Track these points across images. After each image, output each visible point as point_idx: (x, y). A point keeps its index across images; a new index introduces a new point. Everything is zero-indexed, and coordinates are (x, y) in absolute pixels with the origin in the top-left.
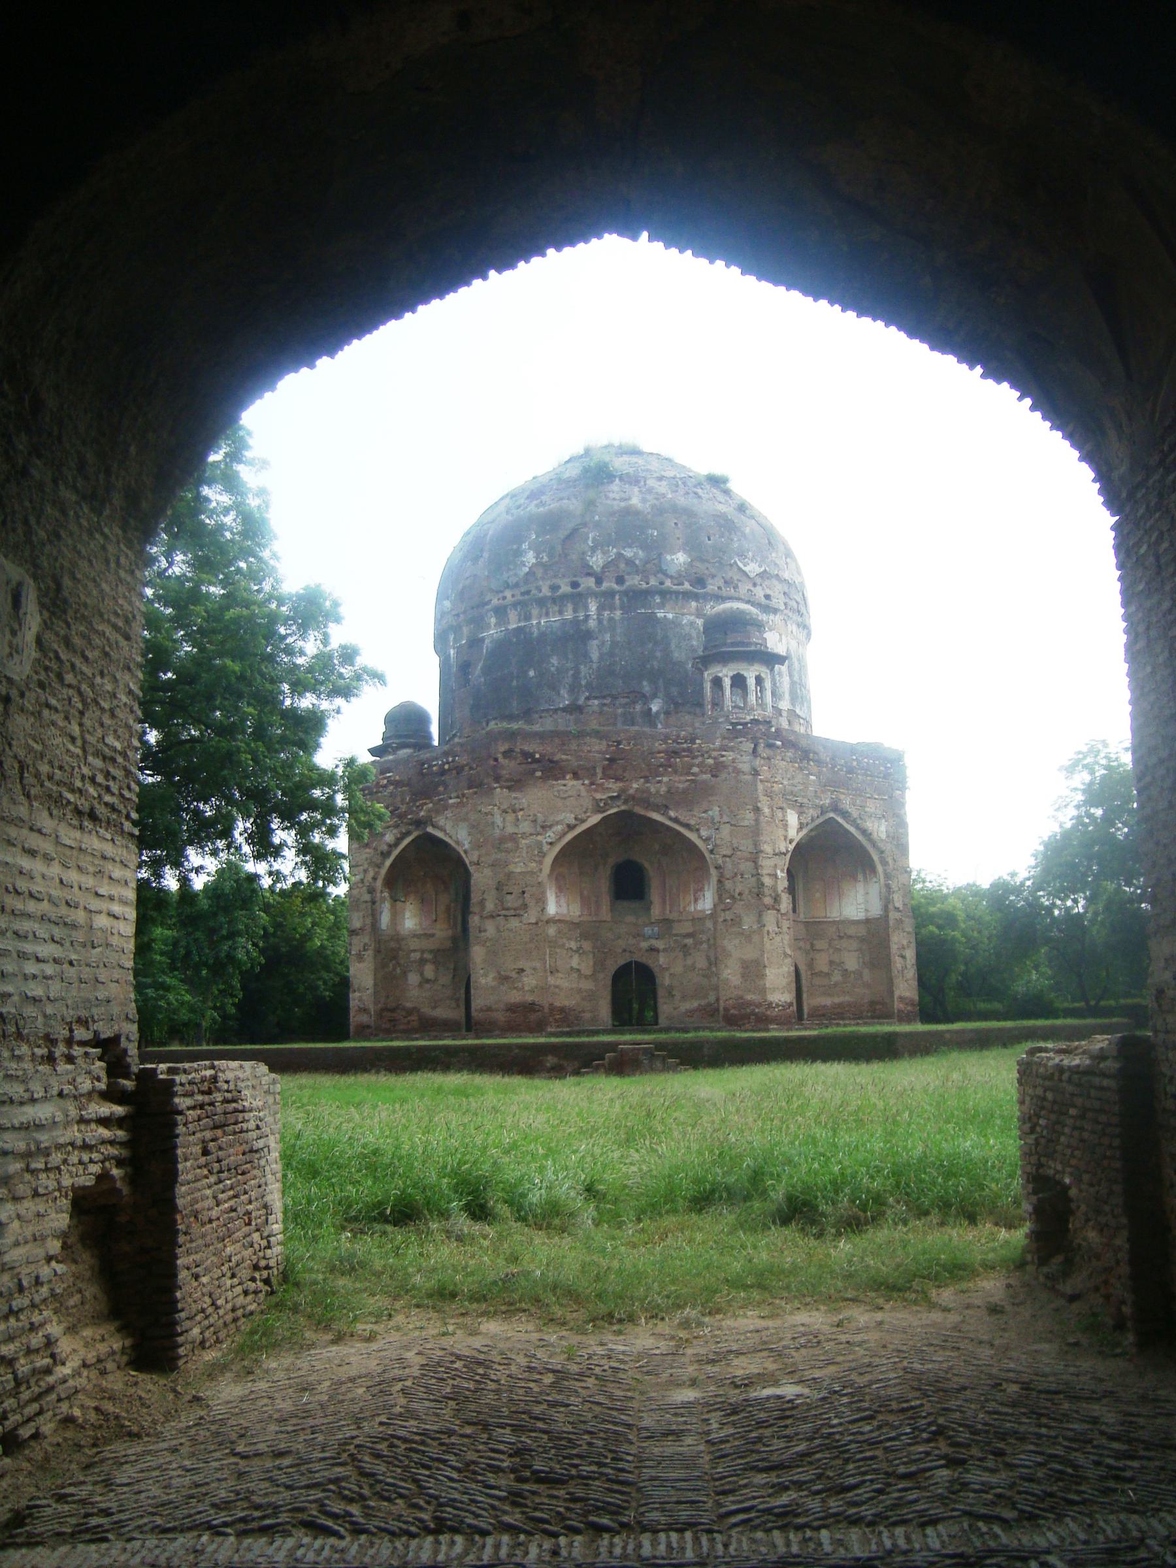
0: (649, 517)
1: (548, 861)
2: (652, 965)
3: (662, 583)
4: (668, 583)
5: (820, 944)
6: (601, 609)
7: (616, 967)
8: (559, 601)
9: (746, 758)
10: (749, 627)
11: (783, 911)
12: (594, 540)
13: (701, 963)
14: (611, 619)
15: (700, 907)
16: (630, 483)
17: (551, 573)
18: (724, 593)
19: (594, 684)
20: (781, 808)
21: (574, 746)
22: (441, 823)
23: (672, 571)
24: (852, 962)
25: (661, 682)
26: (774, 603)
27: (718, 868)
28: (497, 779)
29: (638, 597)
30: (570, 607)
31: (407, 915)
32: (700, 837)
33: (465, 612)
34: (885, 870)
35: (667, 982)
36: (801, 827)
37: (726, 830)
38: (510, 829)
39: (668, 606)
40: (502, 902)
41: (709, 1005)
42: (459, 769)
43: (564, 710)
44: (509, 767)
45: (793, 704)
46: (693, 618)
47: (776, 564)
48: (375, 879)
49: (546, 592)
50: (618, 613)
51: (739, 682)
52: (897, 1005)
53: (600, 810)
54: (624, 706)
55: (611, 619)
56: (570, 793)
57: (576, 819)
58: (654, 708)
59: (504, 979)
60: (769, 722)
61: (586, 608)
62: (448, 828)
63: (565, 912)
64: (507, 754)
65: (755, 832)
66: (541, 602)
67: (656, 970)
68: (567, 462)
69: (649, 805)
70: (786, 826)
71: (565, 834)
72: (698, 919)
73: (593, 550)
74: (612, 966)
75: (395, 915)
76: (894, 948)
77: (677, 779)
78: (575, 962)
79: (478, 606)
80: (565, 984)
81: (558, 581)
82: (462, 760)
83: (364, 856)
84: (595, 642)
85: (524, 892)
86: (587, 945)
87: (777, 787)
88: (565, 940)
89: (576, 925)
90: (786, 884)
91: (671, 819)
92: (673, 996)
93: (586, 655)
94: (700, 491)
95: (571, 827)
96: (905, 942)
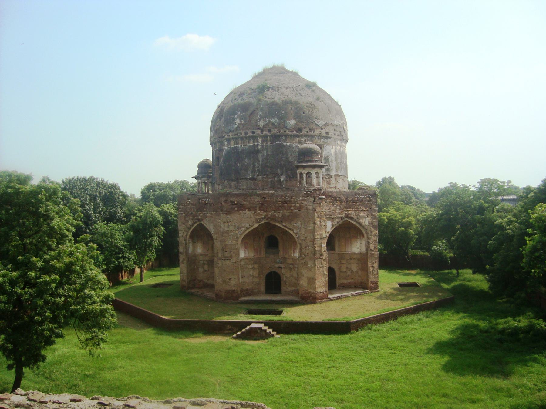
1: (240, 240)
2: (279, 273)
3: (285, 132)
5: (343, 261)
6: (263, 142)
7: (267, 273)
9: (311, 204)
10: (313, 154)
11: (324, 258)
12: (260, 115)
13: (295, 275)
14: (266, 146)
15: (295, 255)
16: (275, 91)
17: (245, 128)
18: (310, 133)
19: (260, 170)
20: (325, 221)
21: (249, 199)
22: (205, 222)
23: (289, 127)
24: (355, 268)
26: (330, 135)
27: (300, 244)
28: (222, 211)
29: (276, 137)
30: (252, 141)
31: (198, 248)
32: (294, 233)
33: (217, 138)
34: (367, 236)
35: (284, 279)
36: (333, 226)
37: (303, 231)
38: (226, 229)
39: (288, 140)
40: (223, 254)
41: (297, 290)
42: (210, 204)
43: (250, 179)
44: (226, 206)
45: (337, 172)
46: (297, 144)
47: (331, 119)
48: (186, 236)
49: (243, 135)
50: (269, 143)
52: (370, 285)
53: (258, 222)
54: (271, 178)
55: (266, 146)
56: (247, 216)
57: (249, 225)
58: (282, 179)
59: (224, 281)
60: (321, 189)
61: (258, 142)
62: (207, 224)
63: (248, 255)
64: (225, 201)
65: (314, 231)
66: (242, 138)
67: (281, 275)
69: (276, 221)
70: (326, 227)
71: (246, 230)
72: (294, 259)
73: (260, 119)
74: (266, 272)
75: (194, 248)
76: (369, 264)
77: (285, 211)
78: (251, 273)
79: (221, 137)
80: (247, 281)
81: (247, 131)
82: (211, 201)
83: (183, 227)
84: (261, 154)
85: (231, 251)
86: (256, 266)
87: (322, 214)
88: (247, 266)
89: (251, 260)
90: (326, 248)
91: (283, 226)
92: (287, 284)
93: (258, 159)
94: (302, 92)
95: (248, 228)
96: (374, 262)
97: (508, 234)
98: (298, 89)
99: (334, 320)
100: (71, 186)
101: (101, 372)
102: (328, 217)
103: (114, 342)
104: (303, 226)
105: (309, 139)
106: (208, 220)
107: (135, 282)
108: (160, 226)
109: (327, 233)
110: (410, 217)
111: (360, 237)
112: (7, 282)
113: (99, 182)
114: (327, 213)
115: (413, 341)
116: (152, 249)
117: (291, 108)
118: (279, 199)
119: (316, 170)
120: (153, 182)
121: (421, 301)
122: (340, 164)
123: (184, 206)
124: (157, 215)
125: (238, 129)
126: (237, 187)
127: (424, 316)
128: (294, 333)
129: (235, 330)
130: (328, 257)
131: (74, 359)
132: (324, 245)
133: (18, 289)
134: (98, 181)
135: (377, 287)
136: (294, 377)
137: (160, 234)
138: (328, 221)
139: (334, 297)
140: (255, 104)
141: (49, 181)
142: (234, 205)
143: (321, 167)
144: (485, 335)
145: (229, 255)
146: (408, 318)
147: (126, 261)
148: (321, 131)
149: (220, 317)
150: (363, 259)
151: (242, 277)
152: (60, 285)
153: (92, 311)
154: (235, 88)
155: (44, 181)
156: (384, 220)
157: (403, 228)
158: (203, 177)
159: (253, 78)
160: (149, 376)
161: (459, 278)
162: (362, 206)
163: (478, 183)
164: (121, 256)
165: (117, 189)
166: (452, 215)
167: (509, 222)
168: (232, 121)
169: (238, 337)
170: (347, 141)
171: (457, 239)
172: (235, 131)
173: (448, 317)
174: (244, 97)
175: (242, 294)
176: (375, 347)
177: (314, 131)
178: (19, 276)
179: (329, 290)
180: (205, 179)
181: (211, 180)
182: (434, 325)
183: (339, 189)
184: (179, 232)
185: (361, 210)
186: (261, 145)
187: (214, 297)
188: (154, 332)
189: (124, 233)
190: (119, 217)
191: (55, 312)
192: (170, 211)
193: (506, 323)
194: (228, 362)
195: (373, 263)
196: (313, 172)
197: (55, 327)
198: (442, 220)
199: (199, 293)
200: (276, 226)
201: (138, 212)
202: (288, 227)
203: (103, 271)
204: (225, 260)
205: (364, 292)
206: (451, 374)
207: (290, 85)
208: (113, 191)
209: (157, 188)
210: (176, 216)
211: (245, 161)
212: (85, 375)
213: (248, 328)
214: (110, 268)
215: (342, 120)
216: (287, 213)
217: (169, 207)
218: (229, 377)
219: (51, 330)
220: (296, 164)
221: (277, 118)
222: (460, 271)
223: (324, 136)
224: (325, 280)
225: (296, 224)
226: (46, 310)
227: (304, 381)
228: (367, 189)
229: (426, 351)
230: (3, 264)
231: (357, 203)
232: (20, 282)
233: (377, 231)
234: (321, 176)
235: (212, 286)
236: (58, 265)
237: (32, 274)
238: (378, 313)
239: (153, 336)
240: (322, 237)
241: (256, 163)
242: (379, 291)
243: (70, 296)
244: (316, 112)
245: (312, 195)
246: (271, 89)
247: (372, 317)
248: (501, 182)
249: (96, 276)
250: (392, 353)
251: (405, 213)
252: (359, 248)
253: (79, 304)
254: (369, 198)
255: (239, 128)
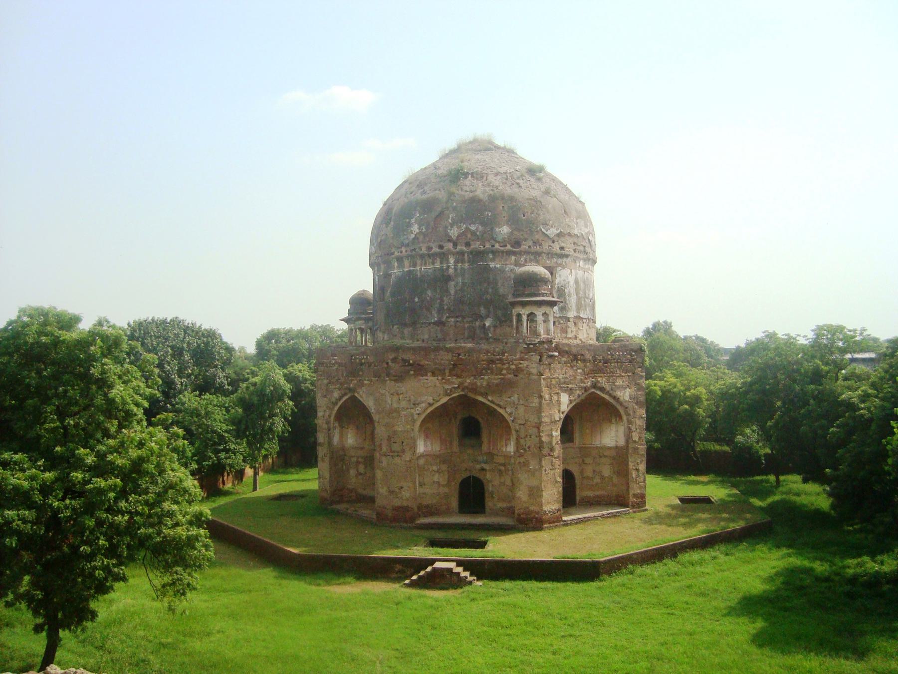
0: (487, 203)
1: (418, 423)
2: (482, 479)
3: (493, 246)
4: (497, 246)
5: (588, 460)
6: (456, 262)
7: (462, 479)
8: (432, 256)
9: (535, 365)
10: (539, 283)
11: (556, 455)
13: (508, 482)
14: (462, 268)
15: (508, 450)
16: (477, 179)
18: (533, 249)
20: (558, 393)
21: (432, 356)
22: (361, 393)
23: (500, 238)
24: (607, 471)
25: (491, 309)
26: (566, 252)
27: (517, 431)
28: (388, 375)
29: (478, 255)
30: (438, 260)
31: (349, 436)
34: (628, 419)
35: (490, 489)
36: (571, 401)
37: (521, 410)
38: (395, 405)
39: (497, 260)
40: (390, 447)
41: (512, 507)
43: (435, 323)
44: (395, 367)
45: (578, 310)
46: (512, 266)
48: (330, 416)
49: (424, 250)
50: (467, 265)
51: (531, 317)
52: (632, 499)
53: (447, 395)
54: (469, 322)
55: (462, 268)
57: (433, 400)
58: (487, 324)
59: (391, 492)
60: (551, 341)
61: (448, 262)
62: (364, 396)
63: (429, 448)
64: (394, 360)
65: (539, 410)
66: (422, 256)
68: (446, 156)
70: (560, 404)
71: (427, 409)
72: (507, 457)
73: (452, 227)
74: (459, 479)
76: (631, 465)
78: (436, 478)
81: (431, 245)
82: (371, 359)
84: (453, 283)
85: (403, 442)
86: (444, 467)
89: (437, 456)
90: (559, 438)
91: (489, 401)
93: (447, 291)
94: (521, 182)
95: (430, 405)
97: (862, 416)
98: (515, 177)
99: (573, 557)
100: (142, 332)
101: (188, 639)
102: (564, 388)
103: (209, 590)
104: (521, 402)
105: (532, 257)
106: (364, 390)
107: (245, 491)
108: (286, 400)
109: (561, 413)
110: (699, 388)
111: (616, 420)
112: (37, 488)
113: (188, 327)
114: (562, 381)
115: (703, 594)
116: (273, 438)
117: (503, 207)
118: (483, 357)
119: (544, 309)
120: (276, 327)
121: (717, 528)
122: (583, 299)
123: (327, 367)
124: (282, 381)
125: (416, 241)
126: (412, 338)
127: (722, 553)
128: (505, 579)
129: (409, 573)
130: (564, 453)
131: (142, 616)
132: (557, 434)
133: (55, 500)
134: (187, 324)
135: (645, 502)
136: (505, 652)
137: (287, 412)
138: (562, 394)
139: (573, 520)
140: (445, 199)
141: (108, 325)
142: (408, 365)
143: (552, 304)
144: (824, 585)
145: (399, 449)
146: (695, 556)
147: (229, 457)
148: (552, 244)
149: (384, 550)
150: (620, 456)
151: (421, 485)
152: (123, 494)
153: (174, 539)
154: (411, 174)
155: (100, 324)
156: (655, 392)
157: (686, 407)
158: (359, 319)
159: (440, 158)
160: (266, 648)
161: (781, 489)
162: (619, 369)
163: (812, 331)
164: (221, 447)
165: (217, 339)
166: (769, 384)
167: (864, 396)
168: (405, 228)
169: (413, 585)
170: (594, 262)
171: (777, 423)
172: (410, 244)
173: (761, 555)
174: (426, 188)
175: (420, 513)
176: (640, 603)
177: (541, 245)
178: (57, 480)
179: (563, 507)
180: (360, 324)
181: (370, 324)
182: (738, 568)
183: (580, 340)
184: (318, 411)
185: (617, 375)
186: (453, 267)
187: (374, 516)
188: (274, 574)
189: (228, 411)
190: (219, 384)
191: (114, 539)
192: (303, 375)
193: (859, 565)
194: (396, 626)
195: (638, 464)
196: (539, 312)
197: (113, 564)
198: (751, 394)
199: (349, 511)
200: (476, 401)
201: (250, 376)
202: (498, 403)
203: (193, 473)
204: (392, 456)
205: (621, 511)
206: (767, 651)
207: (502, 170)
208: (210, 342)
209: (283, 338)
210: (312, 384)
211: (426, 294)
212: (160, 643)
213: (429, 569)
214: (204, 468)
215: (586, 227)
216: (494, 379)
217: (303, 369)
218: (397, 650)
219: (107, 569)
220: (511, 299)
221: (482, 224)
222: (782, 478)
223: (556, 254)
224: (558, 493)
225: (509, 398)
226: (99, 535)
227: (523, 658)
228: (628, 341)
229: (725, 612)
230: (30, 459)
231: (611, 363)
232: (57, 489)
233: (644, 411)
234: (551, 319)
235: (372, 500)
236: (120, 462)
237: (77, 476)
238: (644, 548)
239: (272, 581)
240: (553, 420)
241: (445, 298)
242: (646, 510)
243: (137, 513)
244: (544, 214)
245: (536, 350)
246: (470, 176)
247: (635, 554)
248: (850, 331)
249: (181, 481)
250: (669, 614)
251: (691, 381)
252: (614, 438)
253: (152, 525)
254: (631, 355)
255: (418, 238)
